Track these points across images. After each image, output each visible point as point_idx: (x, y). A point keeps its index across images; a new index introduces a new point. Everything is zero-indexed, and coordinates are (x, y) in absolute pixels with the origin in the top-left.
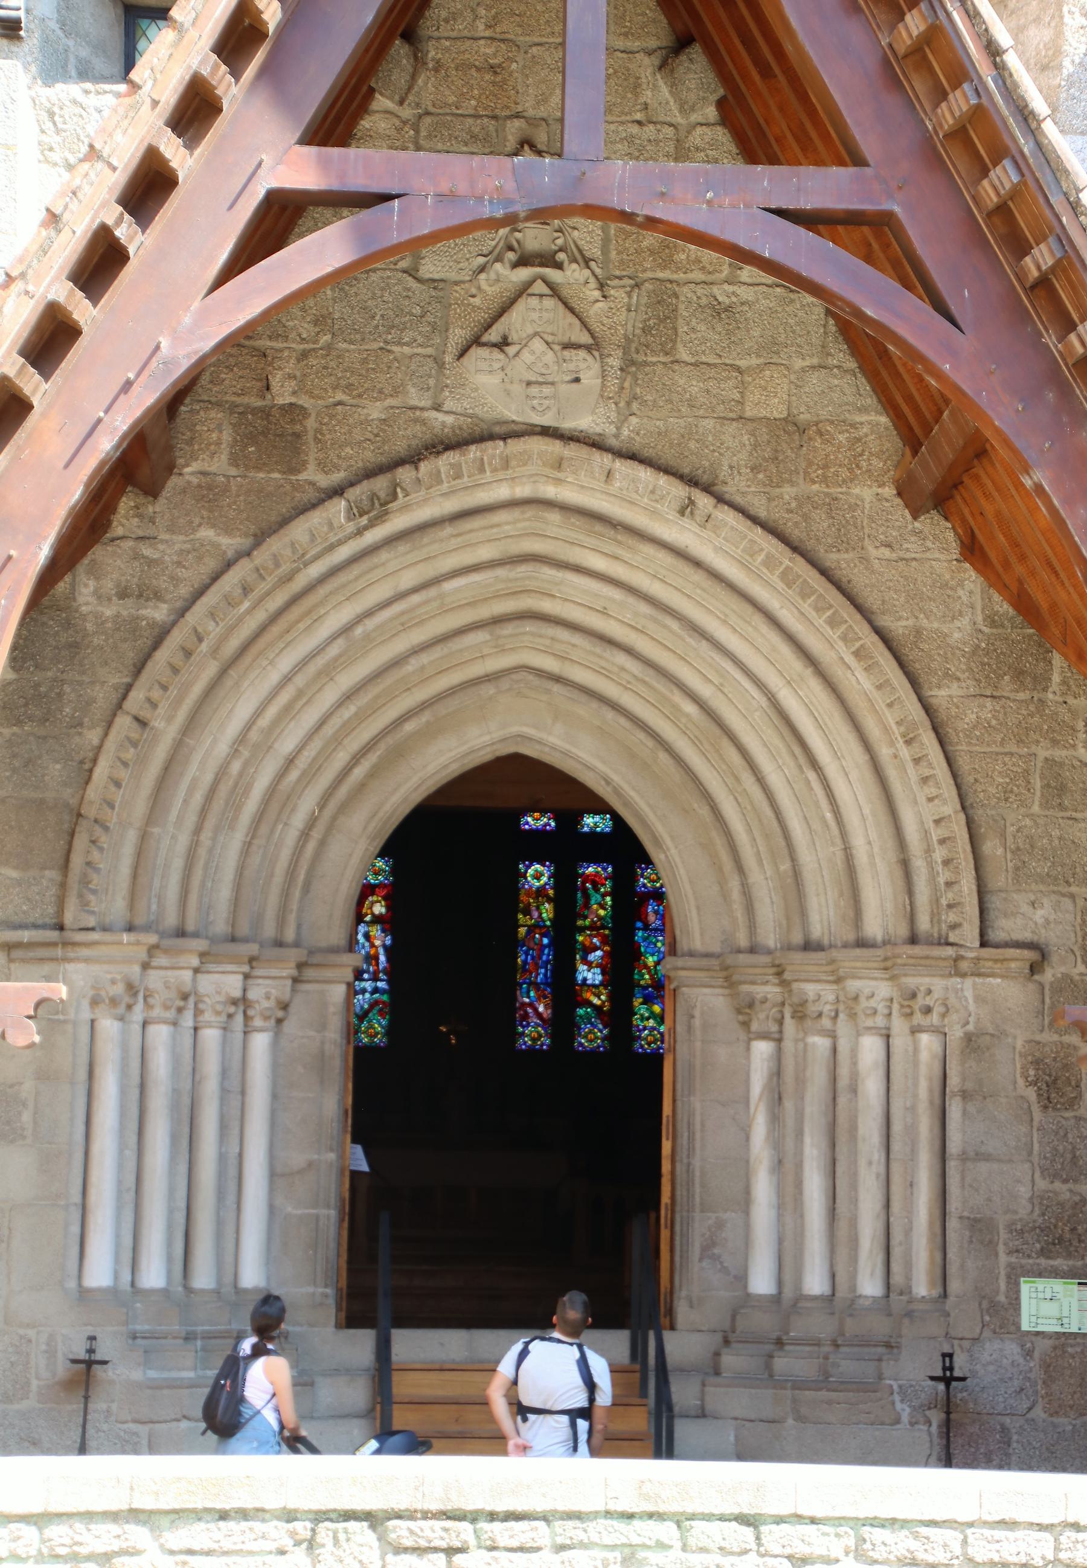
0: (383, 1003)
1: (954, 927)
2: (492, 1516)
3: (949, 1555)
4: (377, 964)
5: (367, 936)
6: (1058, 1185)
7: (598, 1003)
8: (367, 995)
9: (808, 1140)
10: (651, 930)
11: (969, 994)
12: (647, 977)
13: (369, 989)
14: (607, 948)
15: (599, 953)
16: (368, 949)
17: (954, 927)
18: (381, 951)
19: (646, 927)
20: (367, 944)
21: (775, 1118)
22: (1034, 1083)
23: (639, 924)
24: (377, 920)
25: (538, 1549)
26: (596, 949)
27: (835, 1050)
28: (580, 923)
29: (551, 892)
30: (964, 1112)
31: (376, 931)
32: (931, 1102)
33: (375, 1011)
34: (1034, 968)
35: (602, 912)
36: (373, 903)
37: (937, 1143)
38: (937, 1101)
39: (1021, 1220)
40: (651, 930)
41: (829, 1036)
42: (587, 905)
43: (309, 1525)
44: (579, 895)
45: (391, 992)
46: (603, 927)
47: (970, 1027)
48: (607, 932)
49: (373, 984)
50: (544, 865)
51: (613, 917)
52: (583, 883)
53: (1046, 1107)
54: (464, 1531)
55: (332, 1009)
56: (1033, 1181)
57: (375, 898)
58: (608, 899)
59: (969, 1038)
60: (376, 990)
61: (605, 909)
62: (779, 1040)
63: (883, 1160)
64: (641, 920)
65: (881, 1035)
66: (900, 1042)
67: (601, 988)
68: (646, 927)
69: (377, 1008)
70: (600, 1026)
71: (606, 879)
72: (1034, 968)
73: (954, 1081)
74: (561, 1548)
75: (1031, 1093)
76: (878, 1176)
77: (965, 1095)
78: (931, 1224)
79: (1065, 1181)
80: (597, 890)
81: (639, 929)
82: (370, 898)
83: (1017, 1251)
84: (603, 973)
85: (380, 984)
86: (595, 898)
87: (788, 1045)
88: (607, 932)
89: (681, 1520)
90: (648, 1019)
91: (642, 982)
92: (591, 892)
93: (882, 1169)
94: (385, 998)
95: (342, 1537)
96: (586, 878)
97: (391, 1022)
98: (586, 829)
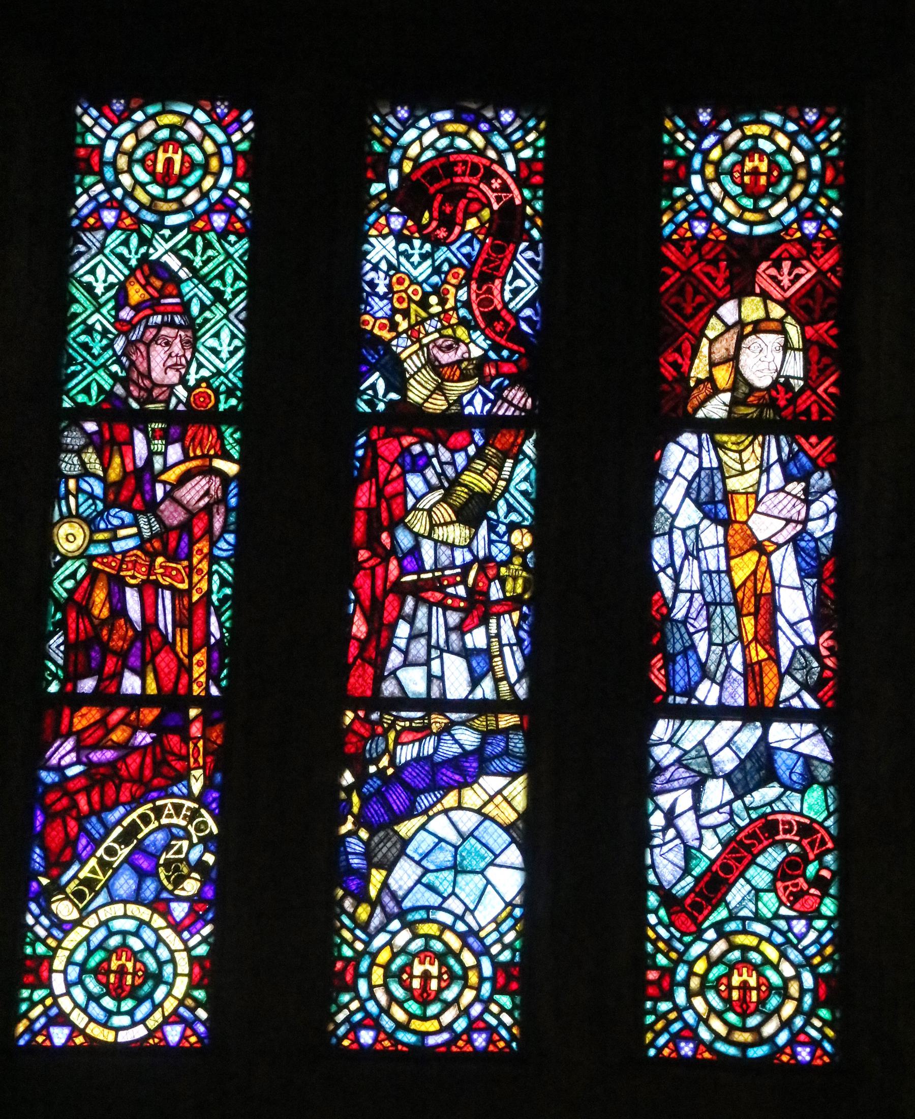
0: (807, 829)
4: (768, 637)
5: (714, 503)
8: (716, 792)
13: (727, 761)
16: (714, 559)
18: (786, 565)
20: (712, 534)
24: (763, 414)
31: (751, 465)
33: (760, 877)
36: (742, 330)
45: (846, 778)
49: (749, 737)
57: (753, 309)
60: (760, 766)
69: (772, 858)
82: (728, 311)
85: (781, 734)
94: (815, 804)
97: (845, 928)
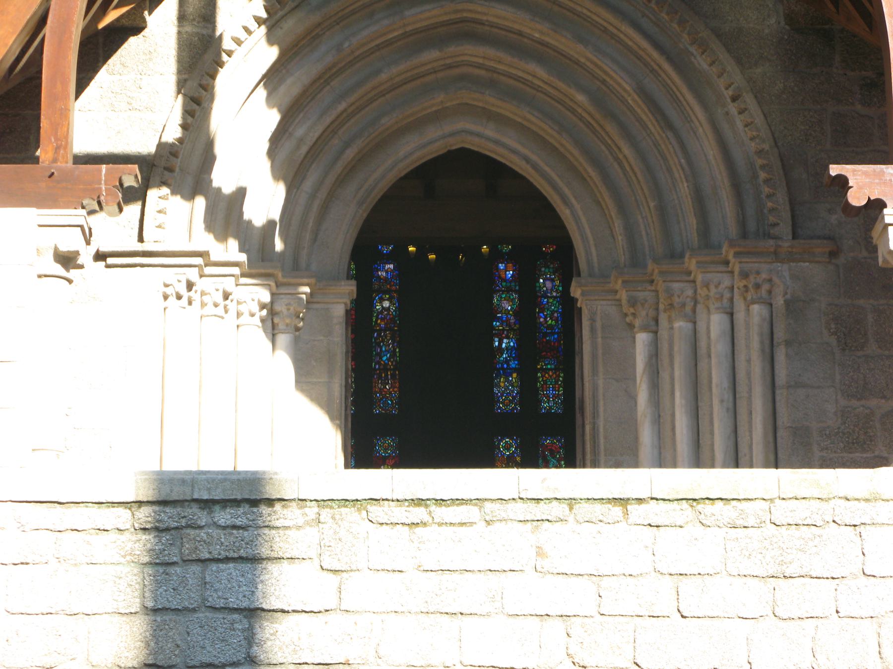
1: (775, 225)
2: (440, 502)
3: (758, 521)
6: (854, 403)
9: (677, 394)
11: (786, 274)
17: (775, 225)
21: (655, 386)
22: (835, 333)
25: (472, 524)
27: (695, 331)
29: (518, 459)
30: (787, 355)
32: (763, 351)
34: (833, 254)
37: (769, 379)
38: (767, 350)
39: (828, 427)
41: (691, 321)
43: (316, 510)
47: (788, 296)
50: (512, 439)
53: (844, 350)
54: (418, 514)
55: (335, 321)
56: (837, 400)
59: (787, 303)
62: (656, 332)
63: (731, 399)
65: (727, 313)
66: (740, 316)
71: (560, 448)
72: (833, 254)
73: (780, 334)
74: (488, 523)
75: (833, 340)
76: (728, 409)
77: (788, 343)
78: (765, 435)
79: (859, 399)
80: (554, 457)
83: (827, 449)
87: (663, 333)
89: (571, 502)
92: (549, 458)
93: (731, 405)
95: (337, 517)
96: (546, 447)
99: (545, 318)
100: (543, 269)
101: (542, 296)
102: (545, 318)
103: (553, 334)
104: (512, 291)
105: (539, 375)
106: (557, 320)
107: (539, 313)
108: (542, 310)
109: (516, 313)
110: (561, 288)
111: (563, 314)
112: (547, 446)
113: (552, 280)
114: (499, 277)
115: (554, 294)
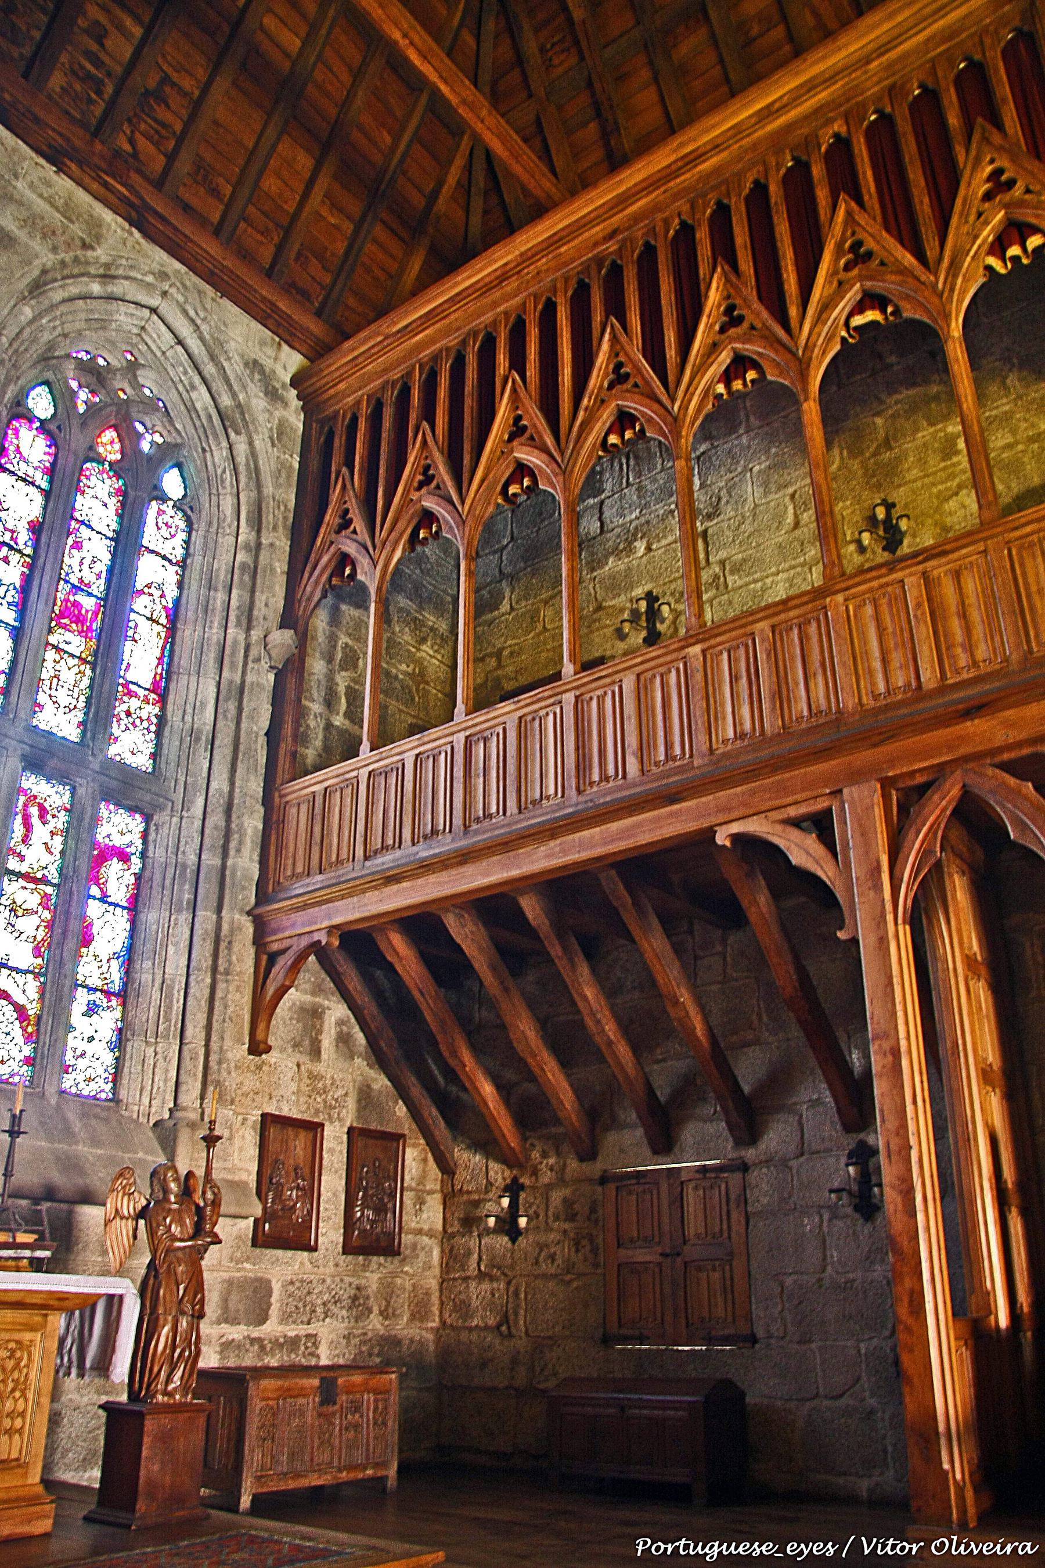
7: (21, 1000)
10: (111, 904)
12: (97, 973)
14: (47, 915)
15: (35, 920)
19: (104, 898)
23: (95, 891)
26: (28, 912)
28: (13, 864)
35: (46, 859)
40: (111, 904)
42: (26, 839)
44: (19, 819)
46: (44, 880)
48: (49, 890)
51: (61, 871)
52: (25, 806)
58: (58, 840)
61: (51, 853)
64: (98, 885)
67: (30, 977)
68: (104, 898)
70: (20, 1039)
80: (44, 823)
81: (94, 898)
84: (37, 952)
86: (40, 832)
88: (49, 890)
90: (91, 1039)
91: (89, 982)
92: (35, 821)
98: (42, 727)
99: (81, 564)
100: (93, 478)
101: (82, 522)
102: (81, 564)
103: (90, 594)
104: (33, 484)
105: (50, 655)
106: (99, 576)
107: (72, 547)
108: (78, 546)
109: (35, 528)
110: (114, 526)
111: (110, 570)
112: (35, 797)
113: (106, 505)
114: (18, 450)
115: (105, 531)
